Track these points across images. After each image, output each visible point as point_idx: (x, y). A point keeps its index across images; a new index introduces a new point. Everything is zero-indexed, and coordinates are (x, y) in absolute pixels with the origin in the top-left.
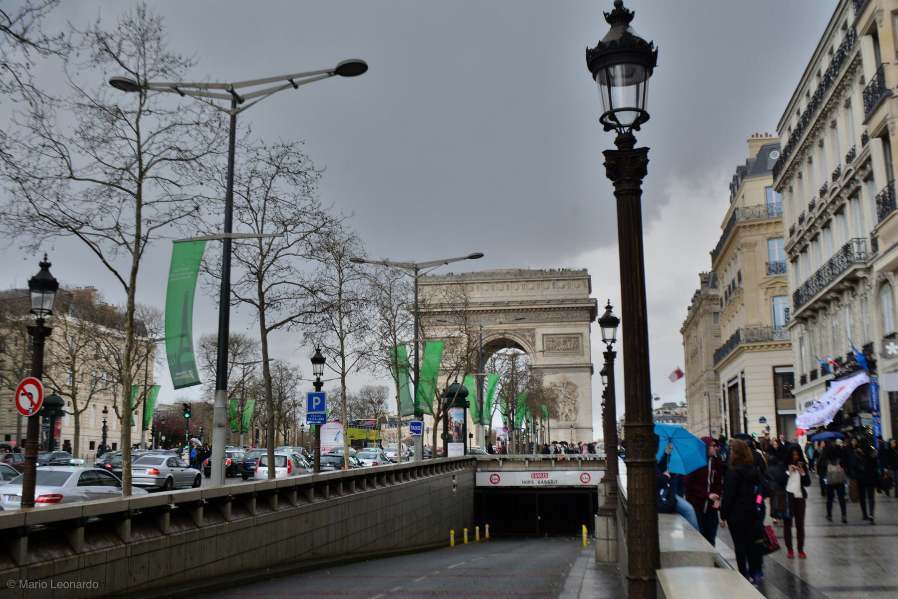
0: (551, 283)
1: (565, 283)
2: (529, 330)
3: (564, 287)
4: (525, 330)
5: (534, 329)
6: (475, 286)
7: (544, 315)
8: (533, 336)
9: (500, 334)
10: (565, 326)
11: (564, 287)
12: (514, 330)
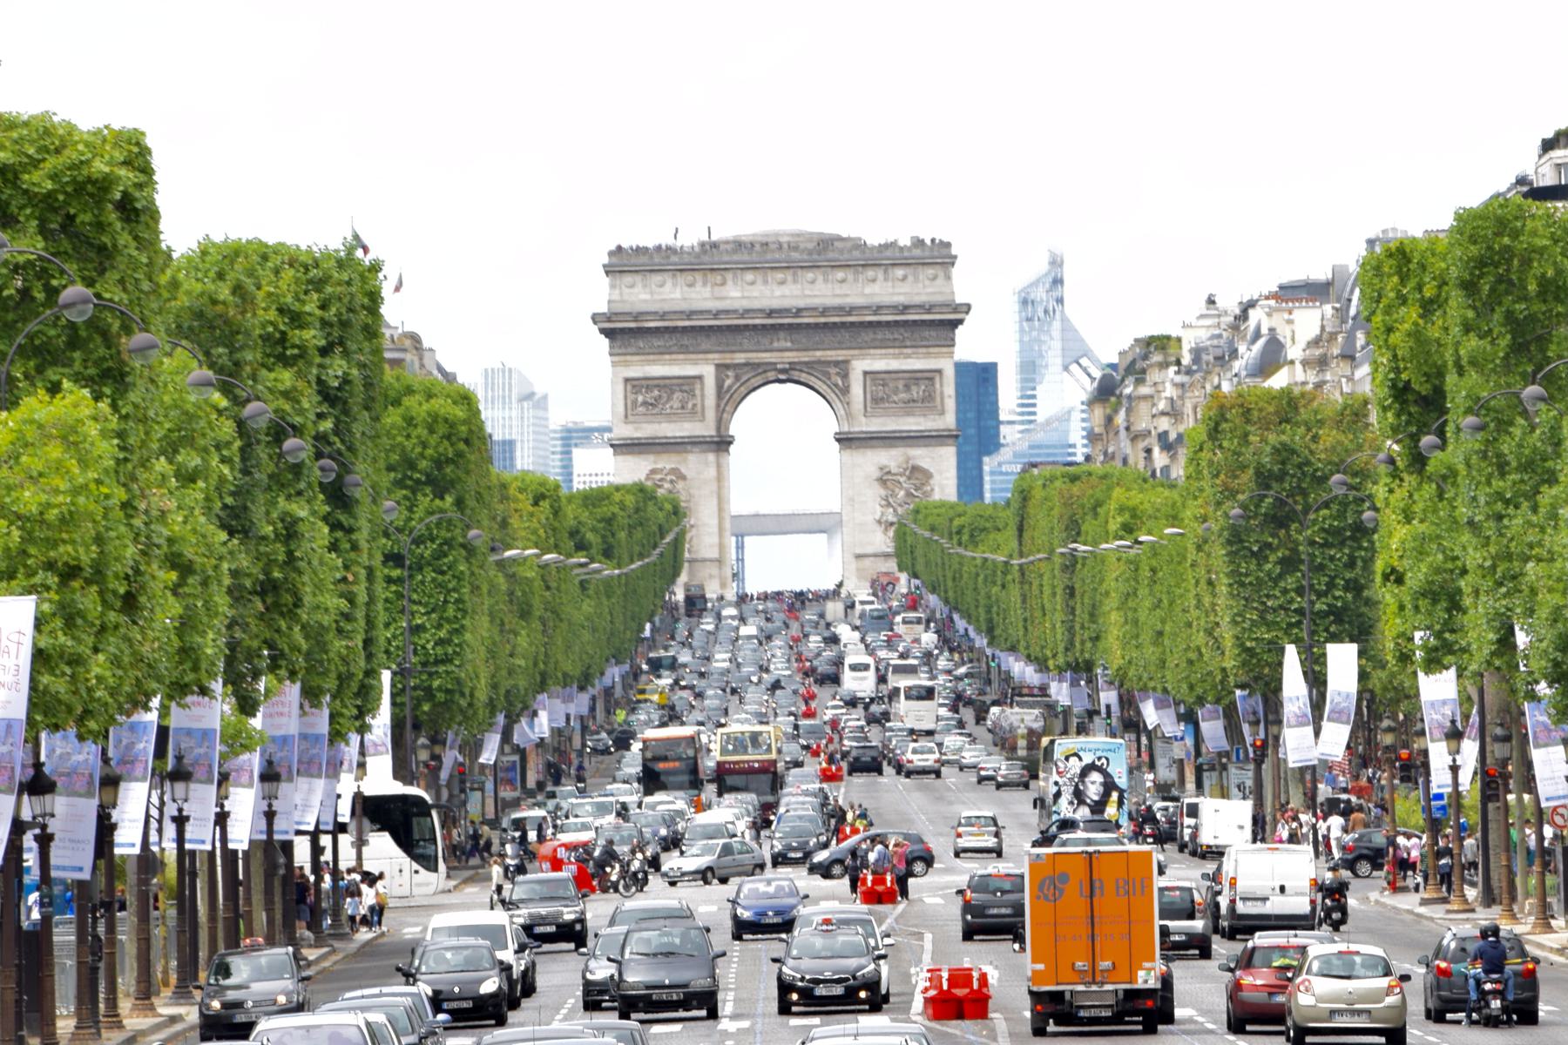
0: (880, 274)
1: (909, 270)
2: (836, 364)
3: (904, 278)
4: (828, 363)
5: (847, 362)
6: (729, 276)
7: (867, 336)
8: (845, 376)
10: (908, 356)
11: (904, 278)
12: (806, 363)
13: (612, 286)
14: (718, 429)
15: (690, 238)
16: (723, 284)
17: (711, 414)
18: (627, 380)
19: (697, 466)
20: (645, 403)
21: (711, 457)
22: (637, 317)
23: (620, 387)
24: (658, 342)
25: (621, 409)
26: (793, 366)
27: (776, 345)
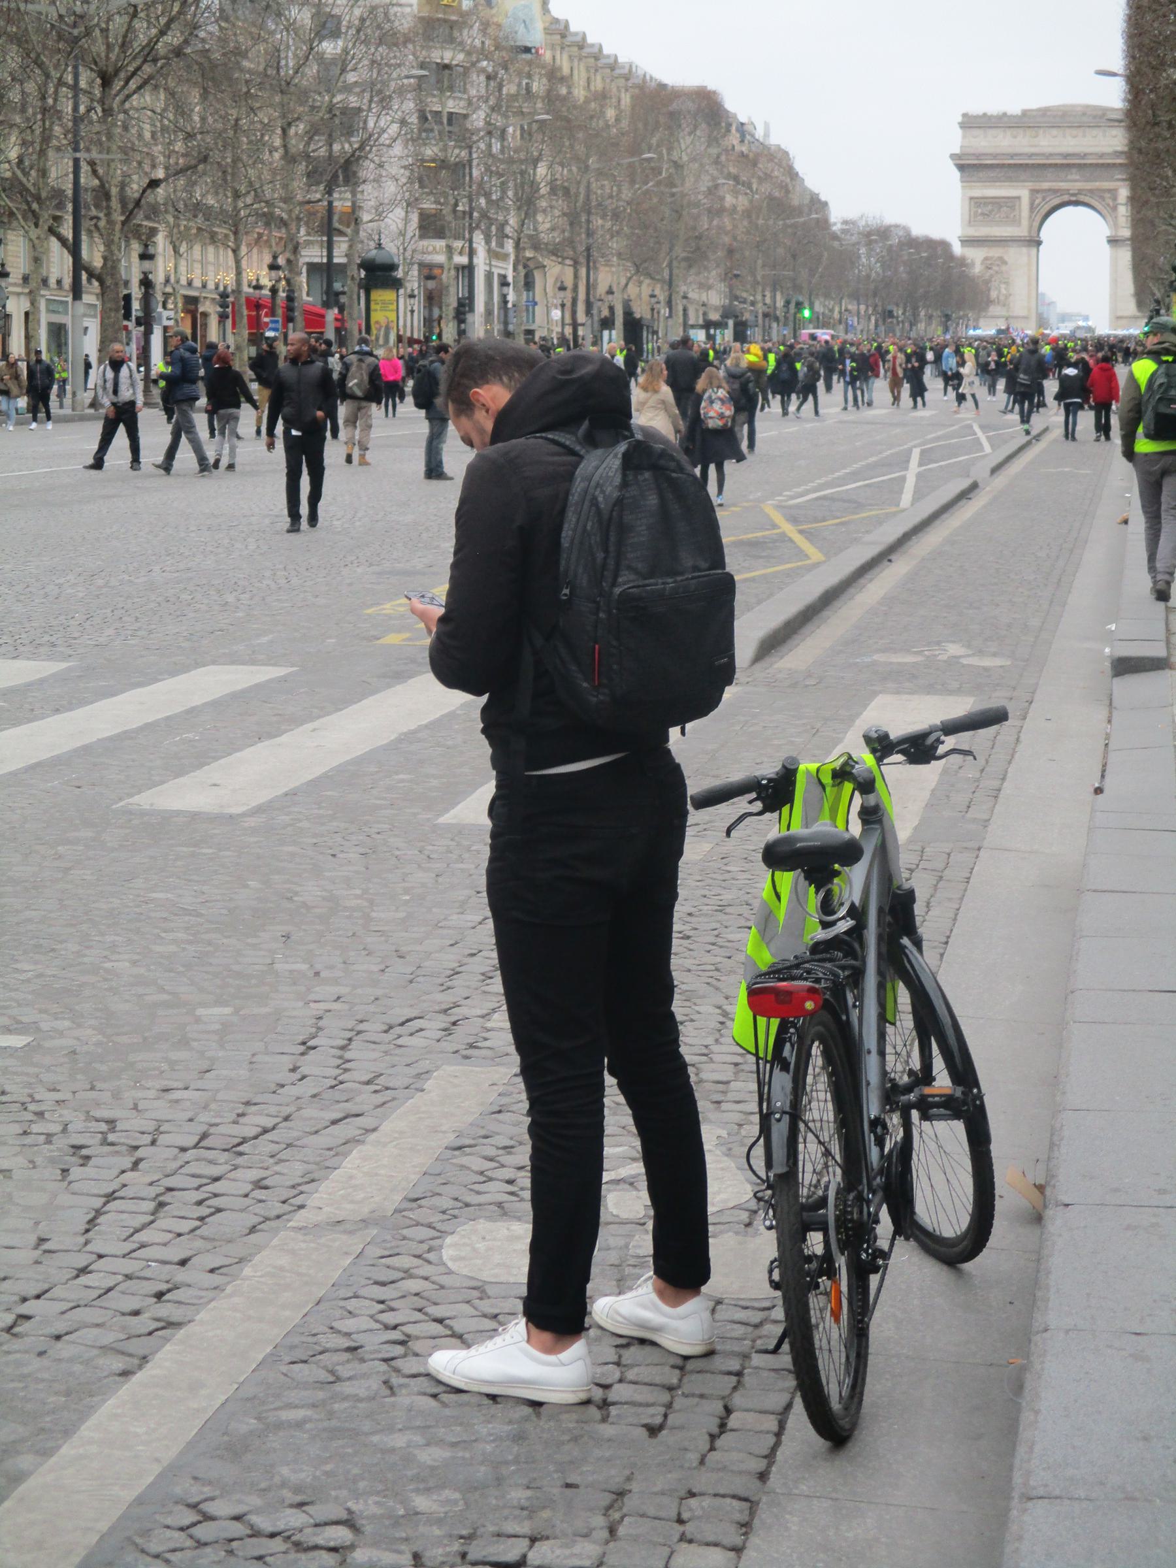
2: (1109, 191)
5: (1116, 190)
6: (1041, 131)
8: (1115, 199)
9: (1073, 195)
12: (1091, 191)
13: (964, 137)
14: (1030, 232)
15: (1014, 108)
16: (1036, 136)
17: (1025, 222)
18: (971, 198)
19: (1016, 256)
20: (982, 214)
21: (1024, 250)
22: (978, 156)
23: (967, 202)
24: (992, 174)
25: (967, 217)
26: (1080, 192)
27: (1069, 177)
